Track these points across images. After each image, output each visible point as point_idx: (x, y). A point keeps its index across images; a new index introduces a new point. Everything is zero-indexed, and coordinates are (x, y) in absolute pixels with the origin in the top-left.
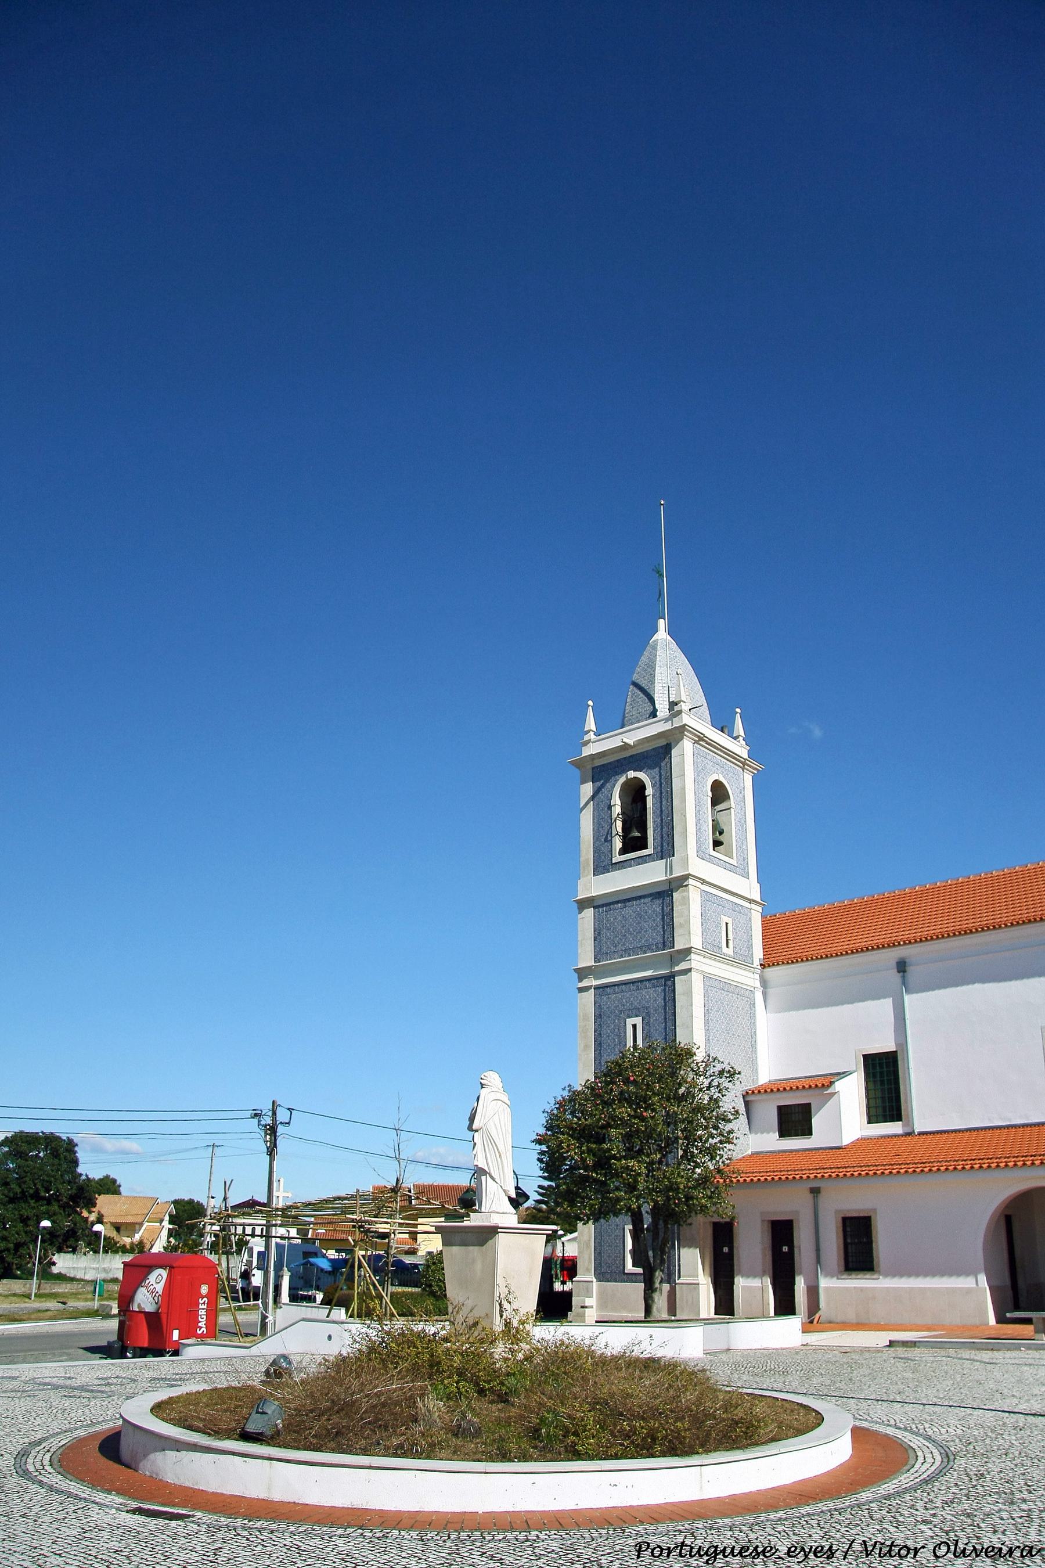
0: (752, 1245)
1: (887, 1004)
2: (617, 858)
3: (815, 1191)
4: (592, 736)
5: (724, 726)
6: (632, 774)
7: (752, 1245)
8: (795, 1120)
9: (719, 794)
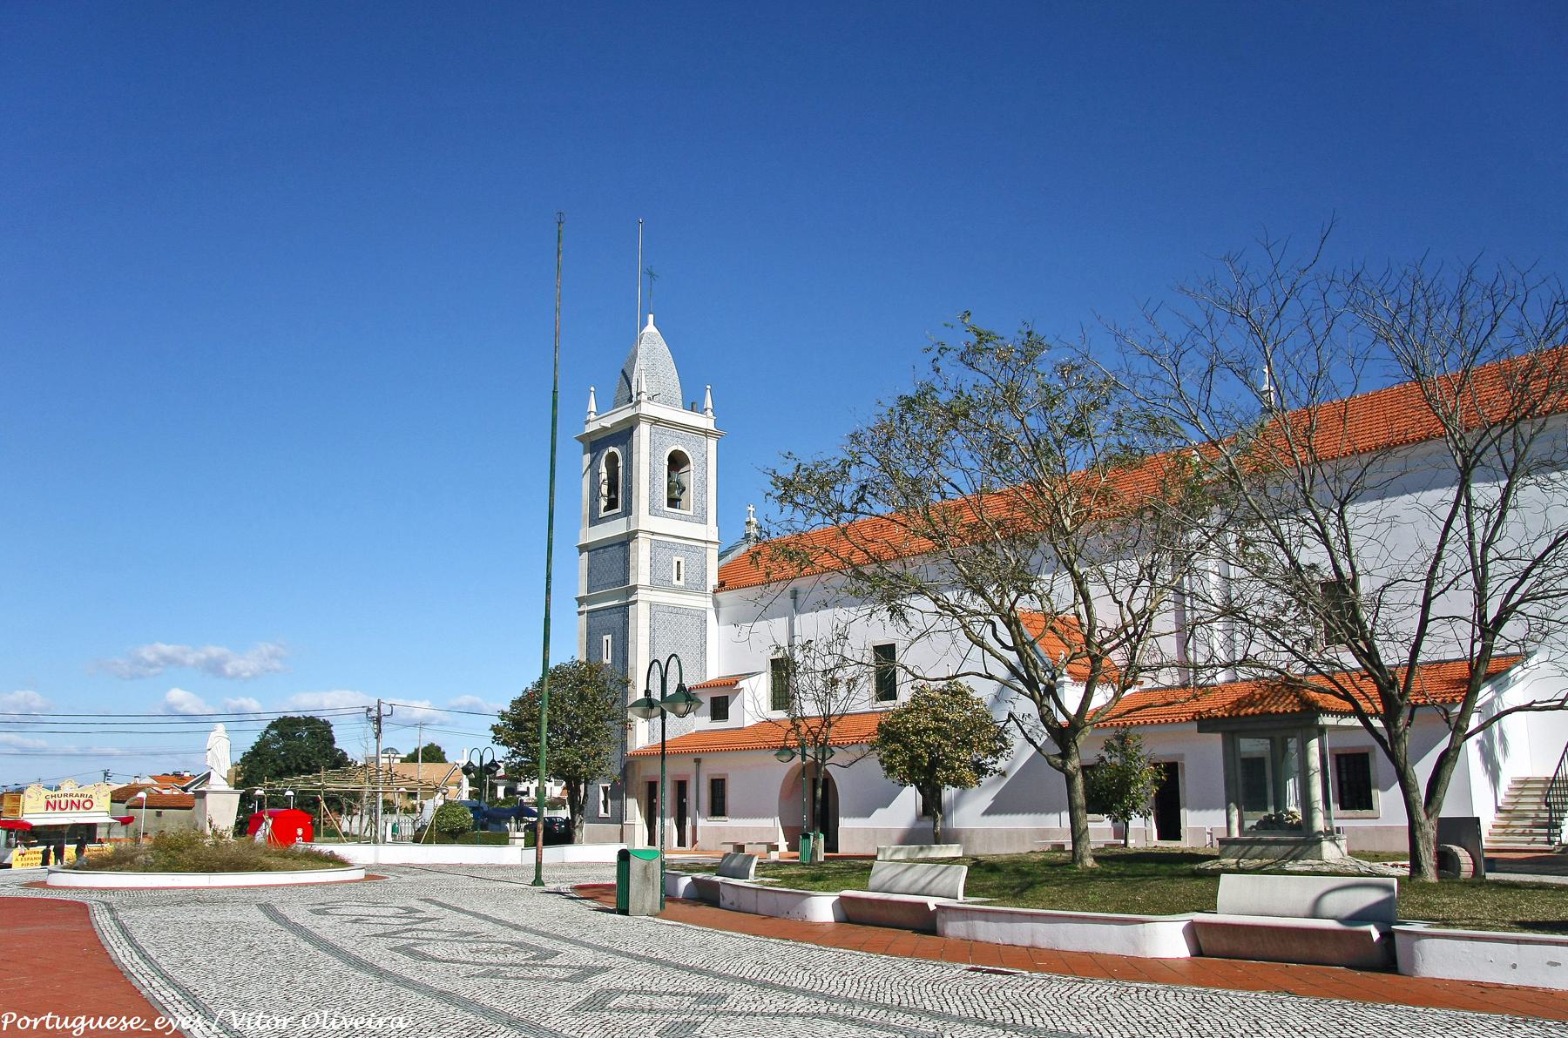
0: (667, 797)
1: (784, 621)
2: (602, 514)
3: (698, 761)
4: (593, 416)
5: (693, 406)
6: (611, 449)
7: (667, 797)
8: (719, 709)
9: (677, 461)
